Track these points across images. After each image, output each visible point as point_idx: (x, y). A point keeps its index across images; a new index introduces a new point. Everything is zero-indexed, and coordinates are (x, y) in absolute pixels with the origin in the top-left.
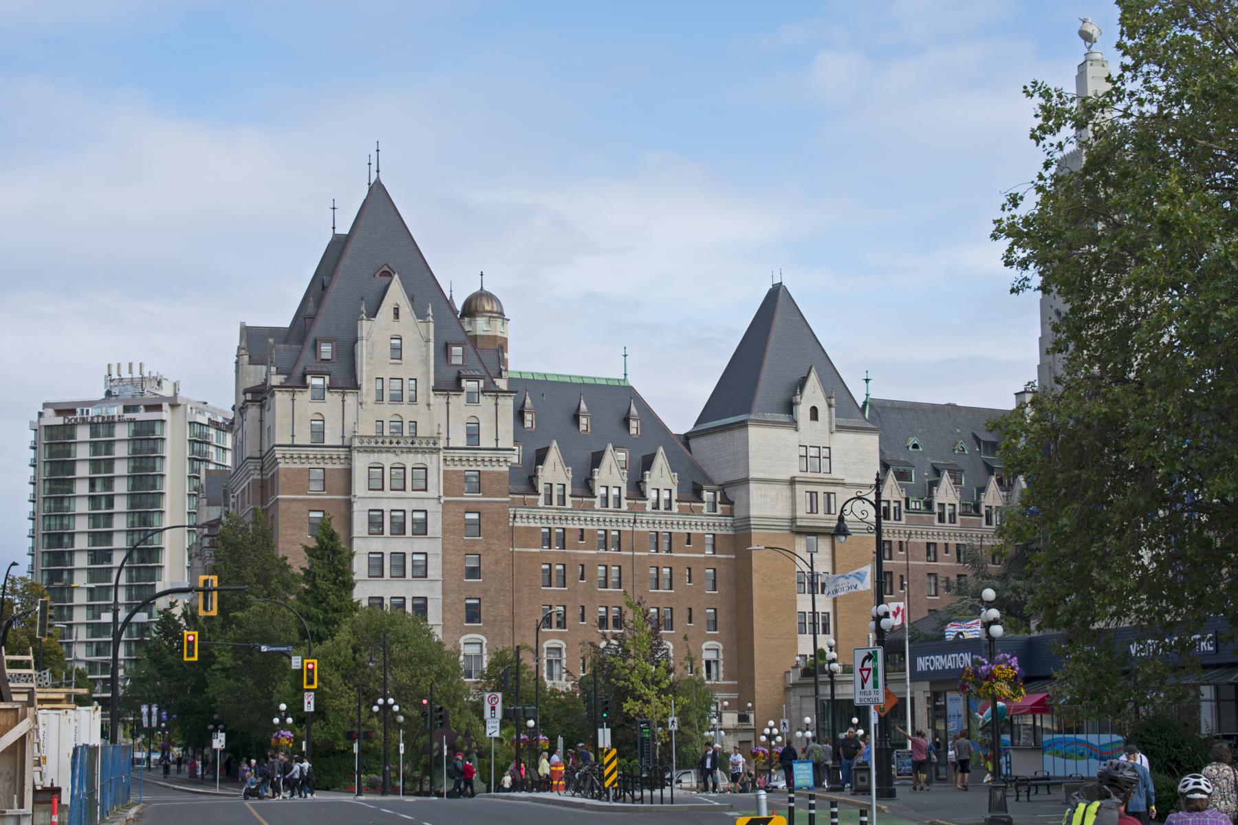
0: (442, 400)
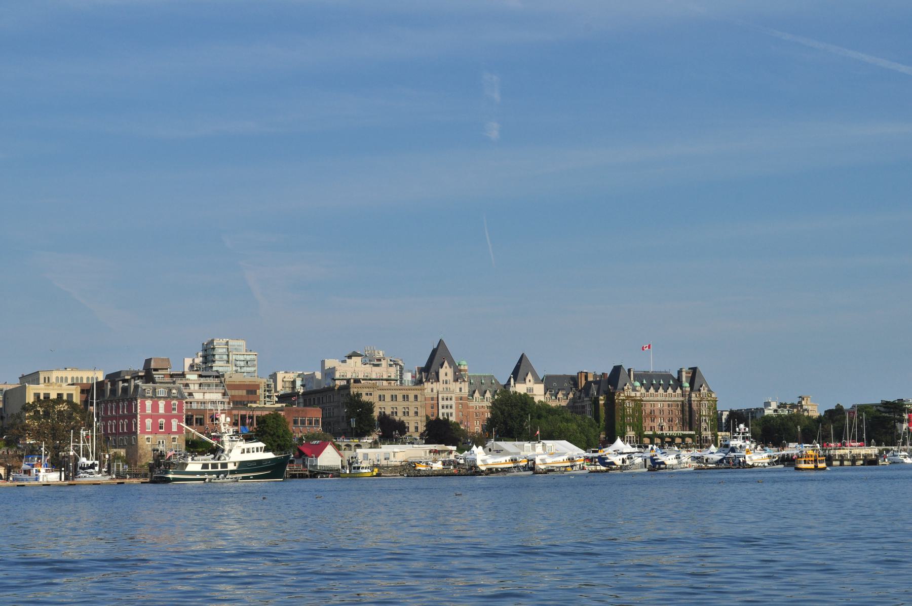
0: (455, 383)
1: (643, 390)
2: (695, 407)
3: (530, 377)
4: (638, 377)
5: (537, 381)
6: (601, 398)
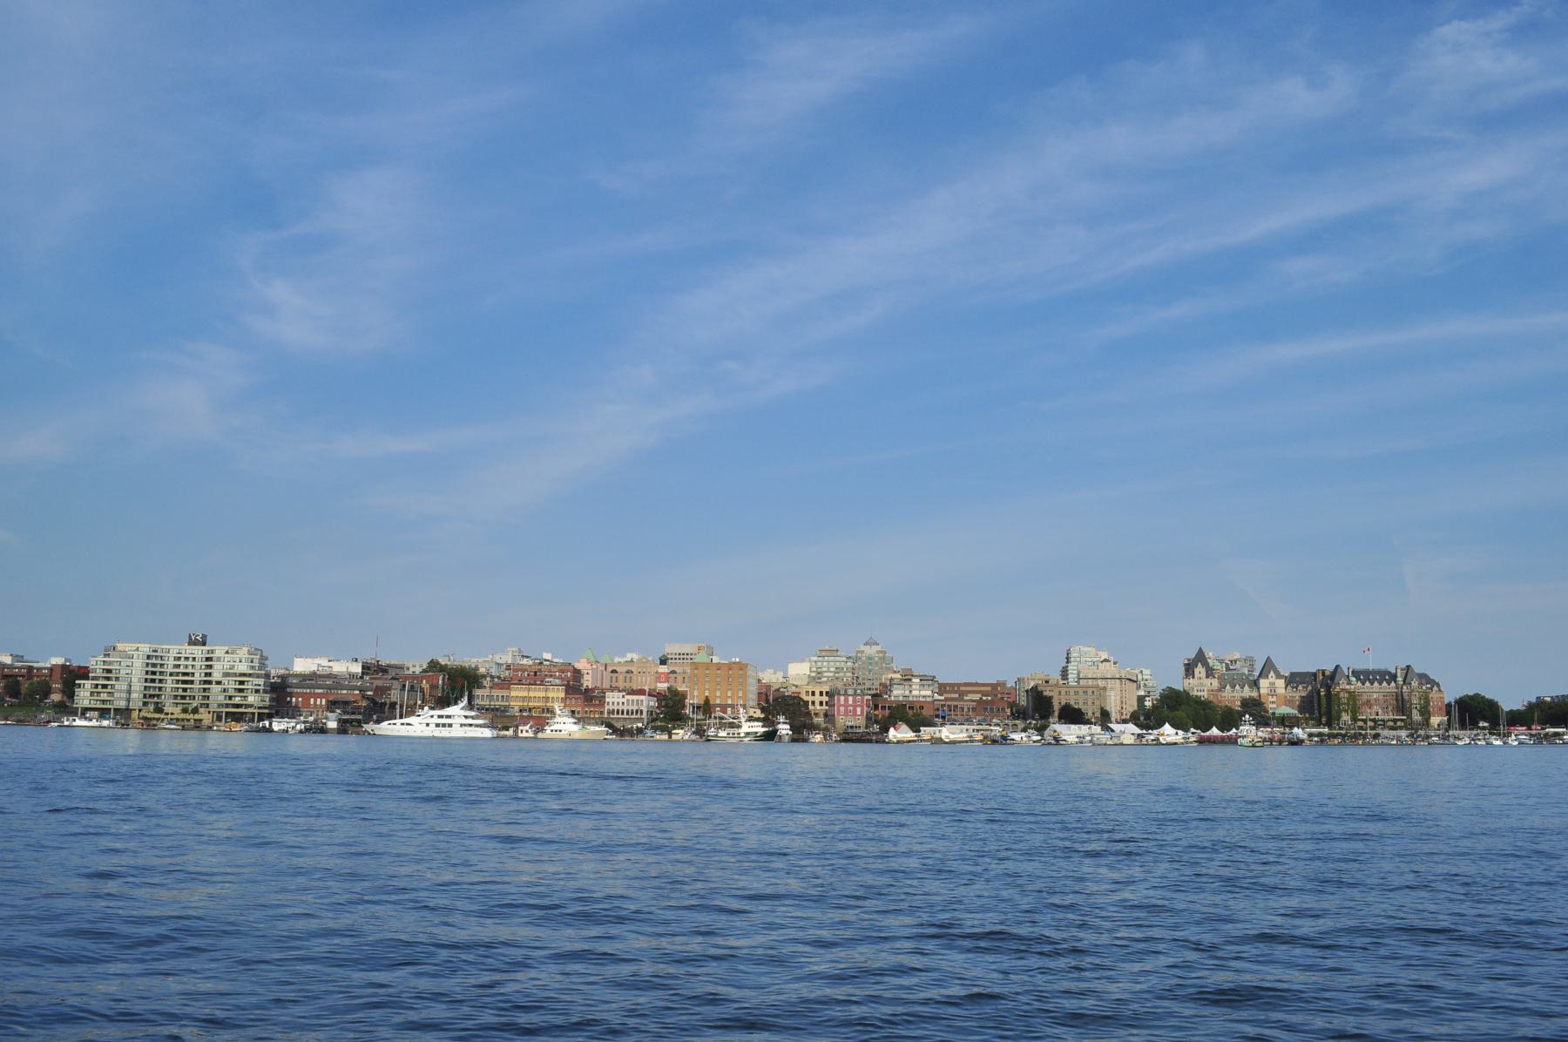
1: (1359, 684)
2: (1406, 698)
3: (1272, 674)
4: (1355, 673)
5: (1279, 676)
6: (1322, 690)
